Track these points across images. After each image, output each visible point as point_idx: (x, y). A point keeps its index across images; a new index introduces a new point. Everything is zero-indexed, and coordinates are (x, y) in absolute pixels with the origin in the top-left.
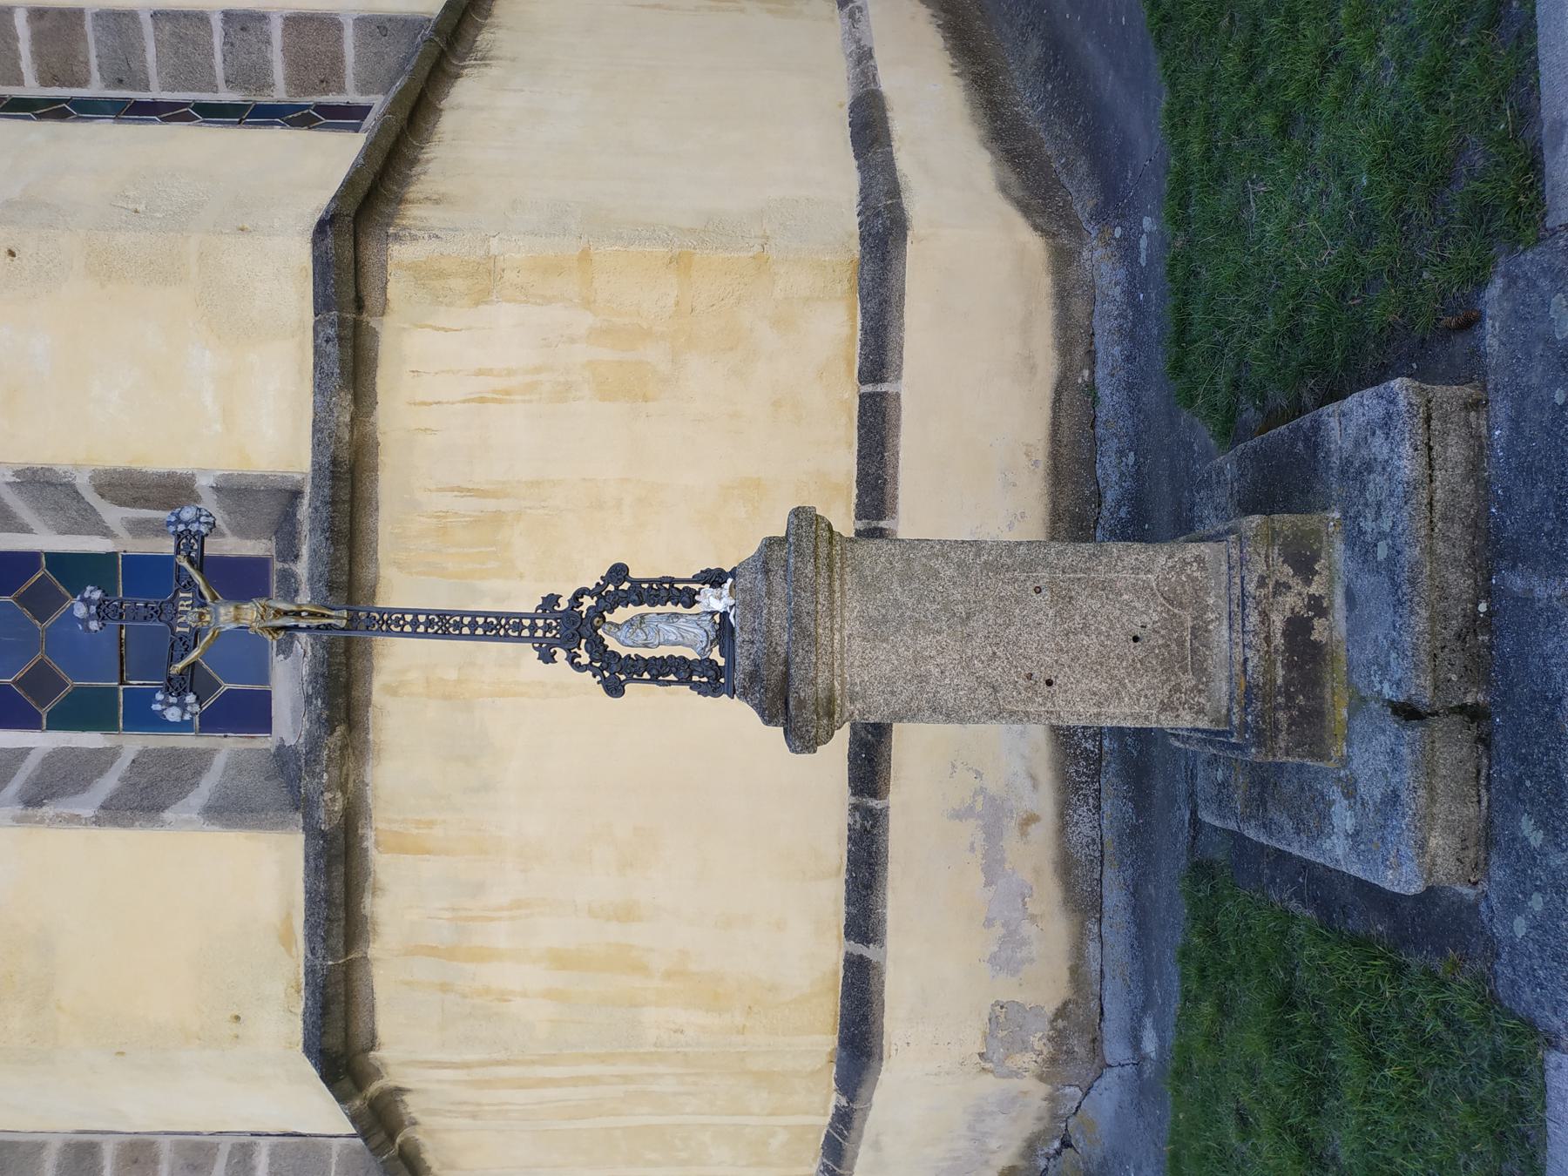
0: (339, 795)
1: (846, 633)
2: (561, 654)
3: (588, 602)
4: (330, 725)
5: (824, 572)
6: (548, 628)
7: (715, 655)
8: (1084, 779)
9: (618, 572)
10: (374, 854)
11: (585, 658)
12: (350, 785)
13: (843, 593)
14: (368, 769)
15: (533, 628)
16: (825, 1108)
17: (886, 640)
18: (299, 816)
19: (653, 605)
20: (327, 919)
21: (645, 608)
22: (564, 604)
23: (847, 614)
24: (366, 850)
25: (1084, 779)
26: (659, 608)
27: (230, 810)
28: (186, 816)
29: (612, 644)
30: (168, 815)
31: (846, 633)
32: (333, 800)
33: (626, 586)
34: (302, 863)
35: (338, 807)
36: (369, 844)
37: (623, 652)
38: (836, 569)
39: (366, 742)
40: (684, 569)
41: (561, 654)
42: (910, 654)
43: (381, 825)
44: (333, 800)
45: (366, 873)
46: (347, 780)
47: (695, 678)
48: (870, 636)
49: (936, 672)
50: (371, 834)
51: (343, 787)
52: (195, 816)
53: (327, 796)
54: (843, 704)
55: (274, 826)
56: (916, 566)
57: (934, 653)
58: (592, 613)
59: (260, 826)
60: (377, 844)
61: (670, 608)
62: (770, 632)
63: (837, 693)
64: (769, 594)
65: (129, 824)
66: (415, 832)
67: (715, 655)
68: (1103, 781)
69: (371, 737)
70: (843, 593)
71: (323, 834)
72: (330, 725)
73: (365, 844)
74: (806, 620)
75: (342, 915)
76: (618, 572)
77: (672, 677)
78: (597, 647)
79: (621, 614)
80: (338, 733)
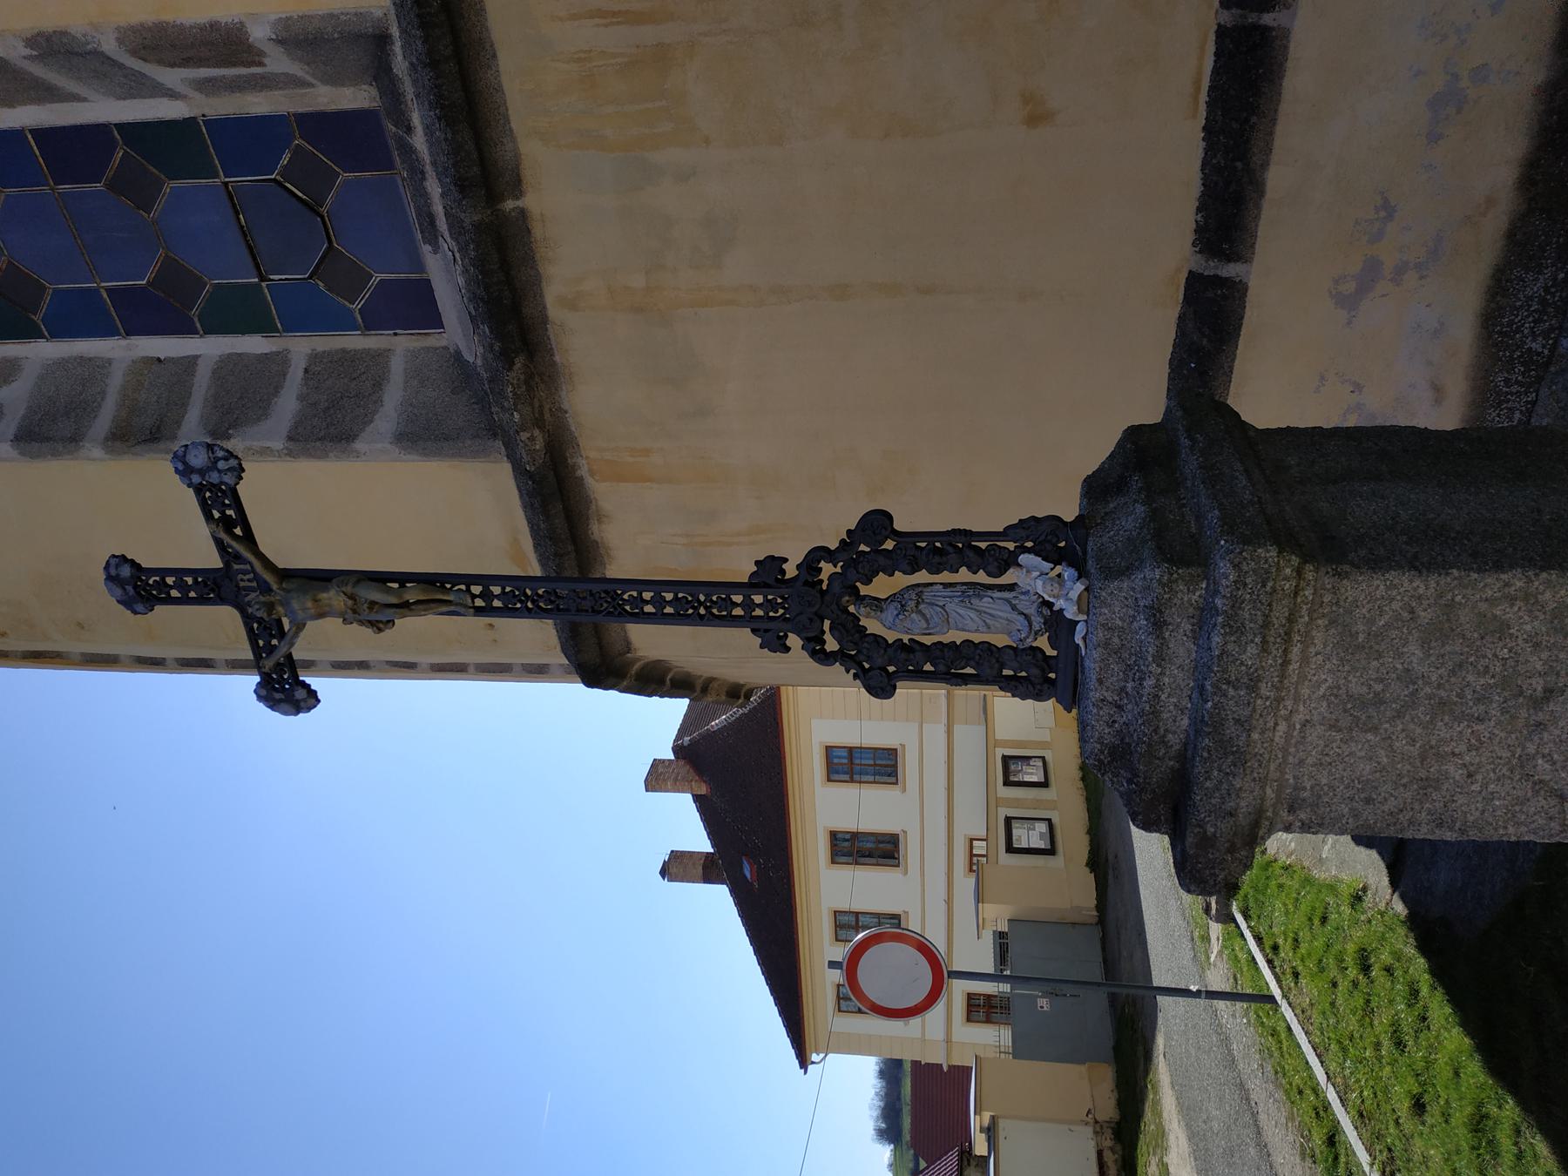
0: (537, 432)
1: (1298, 719)
2: (794, 641)
3: (827, 569)
4: (506, 358)
5: (1276, 651)
6: (769, 605)
7: (1043, 642)
8: (1515, 388)
9: (876, 523)
10: (590, 482)
11: (832, 645)
12: (547, 415)
13: (1305, 660)
14: (563, 394)
15: (748, 605)
16: (1168, 1038)
17: (1375, 730)
18: (499, 444)
19: (935, 570)
20: (556, 555)
21: (922, 576)
22: (791, 570)
23: (1305, 692)
24: (581, 478)
25: (1515, 388)
26: (946, 577)
27: (423, 436)
28: (379, 446)
29: (872, 626)
30: (359, 445)
31: (1298, 719)
32: (532, 439)
33: (889, 545)
34: (516, 492)
35: (539, 445)
36: (583, 472)
37: (891, 637)
38: (1300, 625)
39: (554, 364)
40: (991, 515)
41: (794, 641)
42: (1415, 751)
43: (593, 454)
44: (532, 439)
45: (587, 501)
46: (541, 413)
47: (1006, 672)
48: (1343, 724)
49: (1458, 775)
50: (582, 462)
51: (539, 423)
52: (389, 446)
53: (524, 436)
54: (1275, 813)
55: (475, 455)
56: (1465, 617)
57: (1462, 748)
58: (837, 588)
59: (459, 454)
60: (592, 473)
61: (964, 575)
62: (1155, 713)
63: (1268, 803)
64: (1160, 658)
65: (324, 455)
66: (631, 460)
67: (1043, 642)
68: (1544, 391)
69: (557, 358)
70: (1305, 660)
71: (530, 475)
72: (506, 358)
73: (579, 473)
74: (1231, 730)
75: (571, 548)
76: (876, 523)
77: (969, 670)
78: (850, 629)
79: (882, 586)
80: (518, 366)
